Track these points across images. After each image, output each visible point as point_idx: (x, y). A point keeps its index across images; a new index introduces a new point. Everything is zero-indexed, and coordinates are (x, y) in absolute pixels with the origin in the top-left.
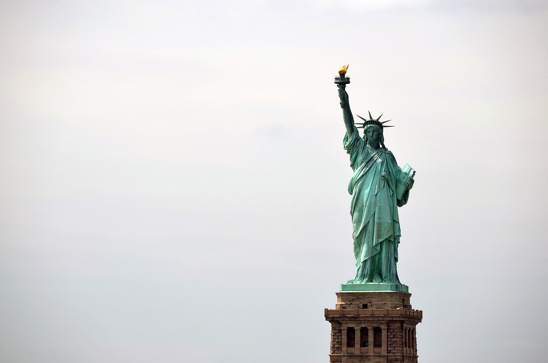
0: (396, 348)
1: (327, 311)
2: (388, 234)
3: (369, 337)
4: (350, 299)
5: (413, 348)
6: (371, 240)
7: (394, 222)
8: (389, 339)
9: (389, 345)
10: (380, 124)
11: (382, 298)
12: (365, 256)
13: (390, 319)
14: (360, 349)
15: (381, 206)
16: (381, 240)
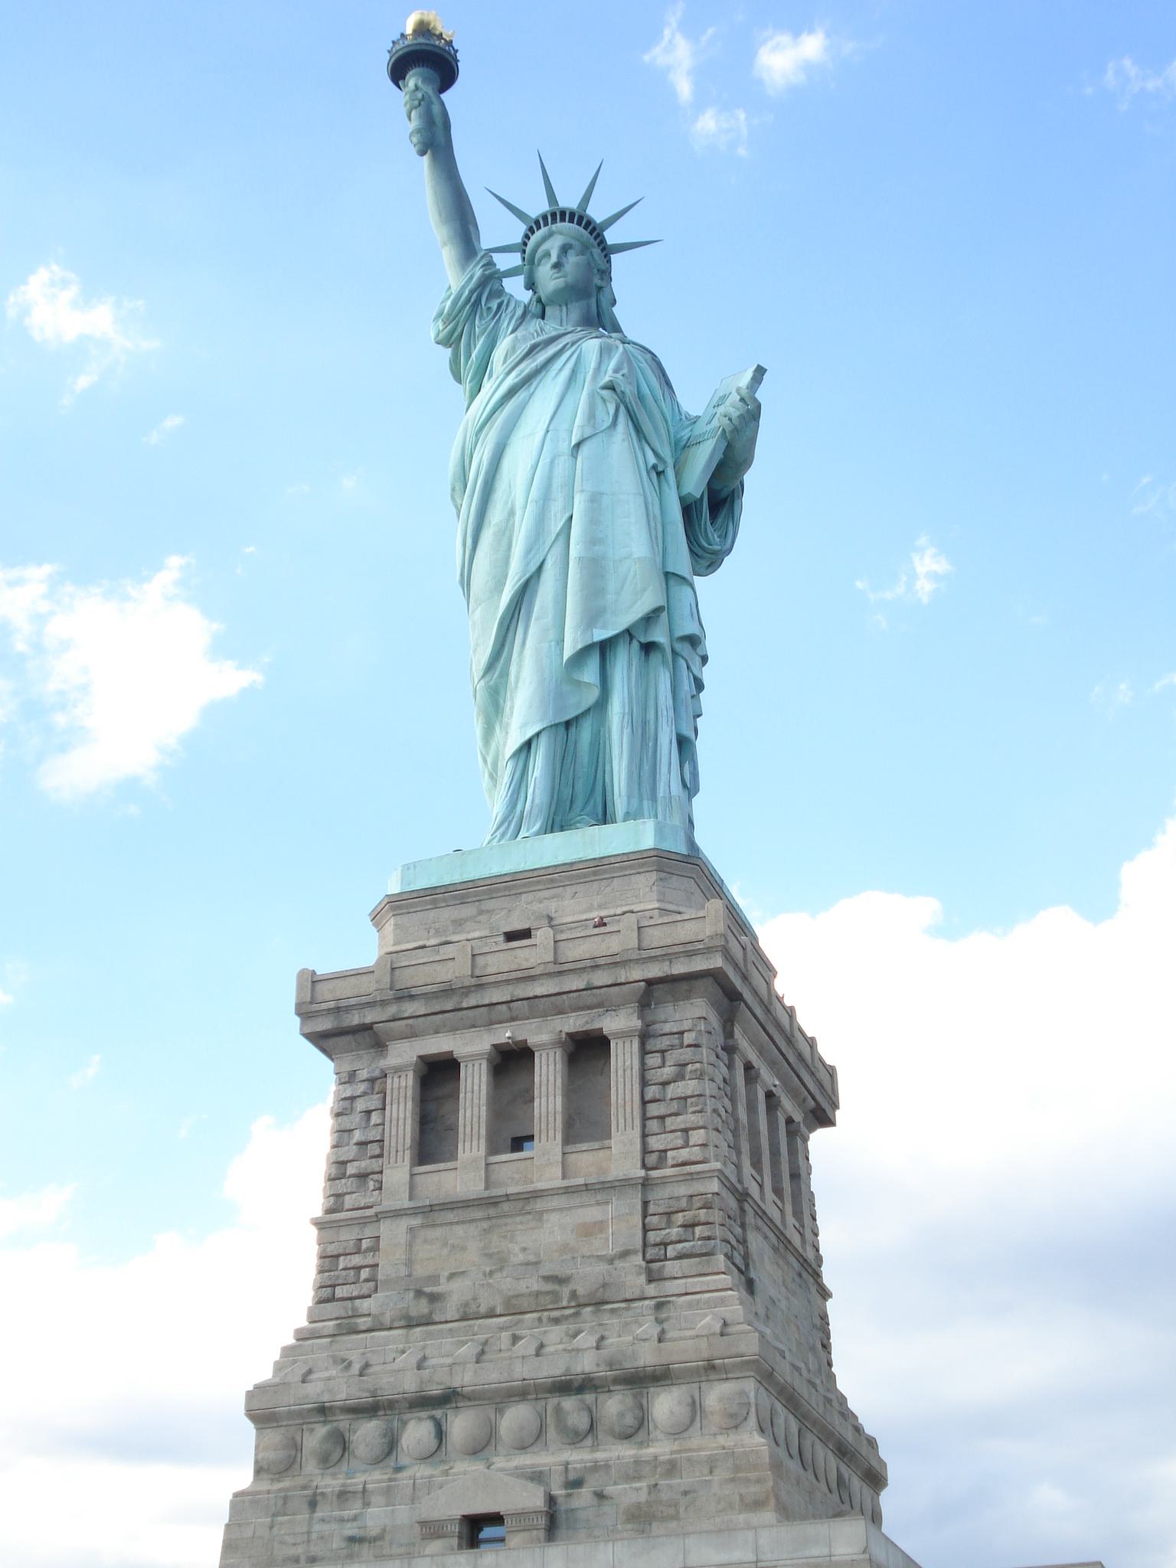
0: (697, 1137)
1: (311, 981)
2: (639, 602)
3: (536, 1093)
4: (437, 925)
5: (798, 1214)
6: (553, 643)
7: (672, 582)
8: (652, 1092)
9: (654, 1125)
10: (594, 229)
11: (608, 889)
12: (524, 726)
13: (655, 971)
14: (487, 1165)
15: (602, 494)
16: (600, 635)
